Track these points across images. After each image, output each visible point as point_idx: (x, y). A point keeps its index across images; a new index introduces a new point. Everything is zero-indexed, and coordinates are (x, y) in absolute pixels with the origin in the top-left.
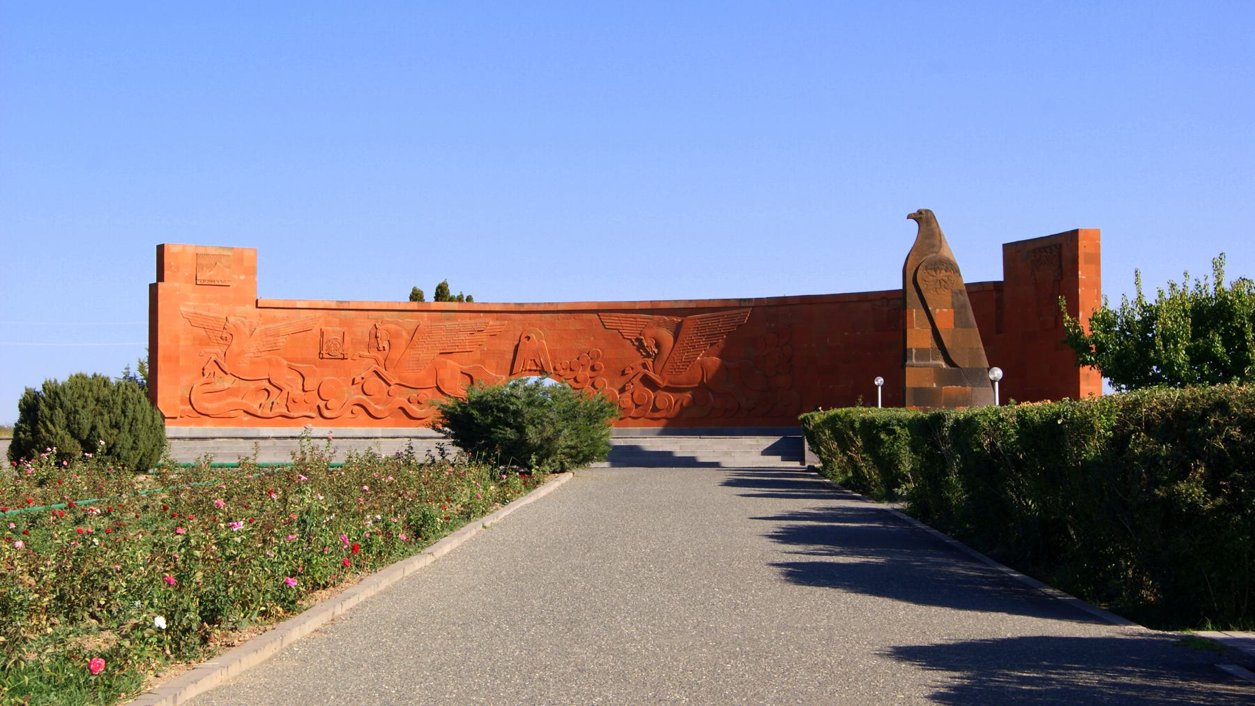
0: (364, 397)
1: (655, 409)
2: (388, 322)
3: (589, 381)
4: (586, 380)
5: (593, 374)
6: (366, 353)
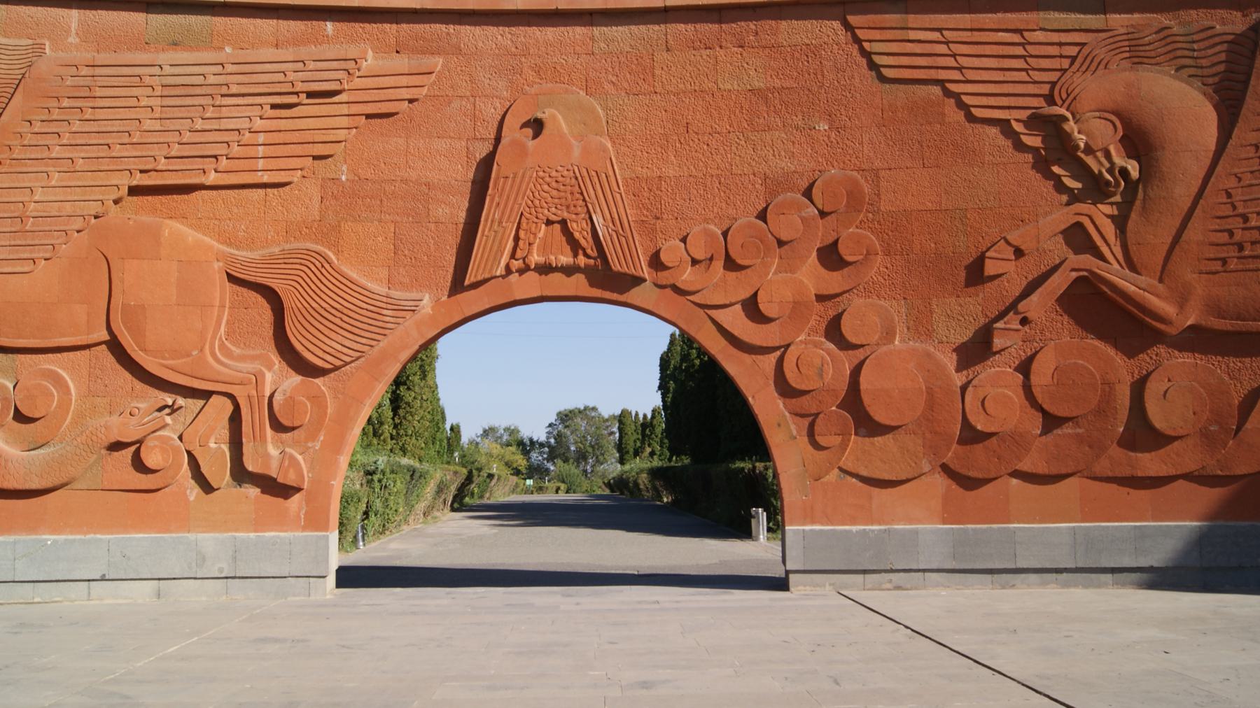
1: (1142, 434)
3: (818, 316)
4: (797, 310)
5: (834, 281)
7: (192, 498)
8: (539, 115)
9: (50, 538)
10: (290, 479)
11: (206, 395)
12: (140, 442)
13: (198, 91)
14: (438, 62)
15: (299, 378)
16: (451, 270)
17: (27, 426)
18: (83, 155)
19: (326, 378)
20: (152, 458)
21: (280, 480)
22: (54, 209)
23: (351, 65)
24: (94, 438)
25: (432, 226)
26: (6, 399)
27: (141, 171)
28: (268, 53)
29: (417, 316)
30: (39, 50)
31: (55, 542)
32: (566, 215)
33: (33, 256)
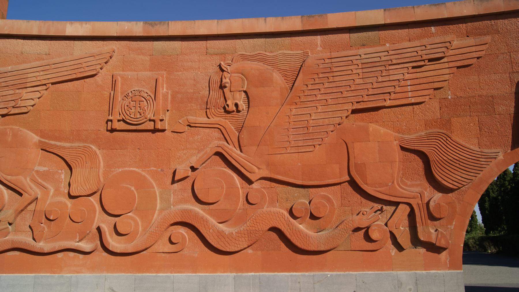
0: (197, 208)
2: (244, 57)
6: (205, 120)
7: (393, 254)
9: (329, 274)
10: (442, 243)
11: (397, 204)
12: (368, 228)
13: (378, 64)
14: (488, 38)
15: (440, 195)
16: (511, 137)
17: (316, 221)
18: (331, 97)
19: (453, 194)
20: (374, 235)
21: (437, 244)
22: (321, 122)
23: (448, 44)
24: (347, 226)
25: (497, 116)
26: (306, 209)
27: (357, 102)
28: (407, 44)
29: (497, 160)
30: (306, 55)
31: (331, 275)
33: (314, 143)
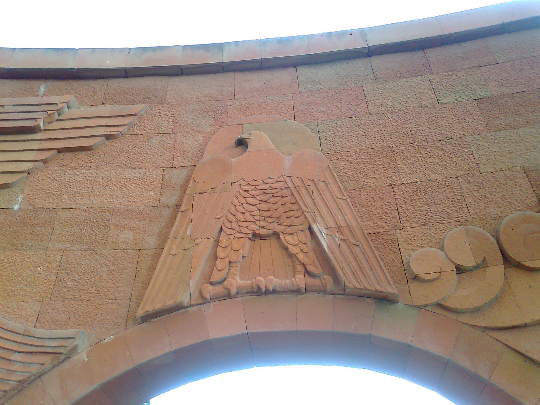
8: (243, 136)
32: (278, 228)
